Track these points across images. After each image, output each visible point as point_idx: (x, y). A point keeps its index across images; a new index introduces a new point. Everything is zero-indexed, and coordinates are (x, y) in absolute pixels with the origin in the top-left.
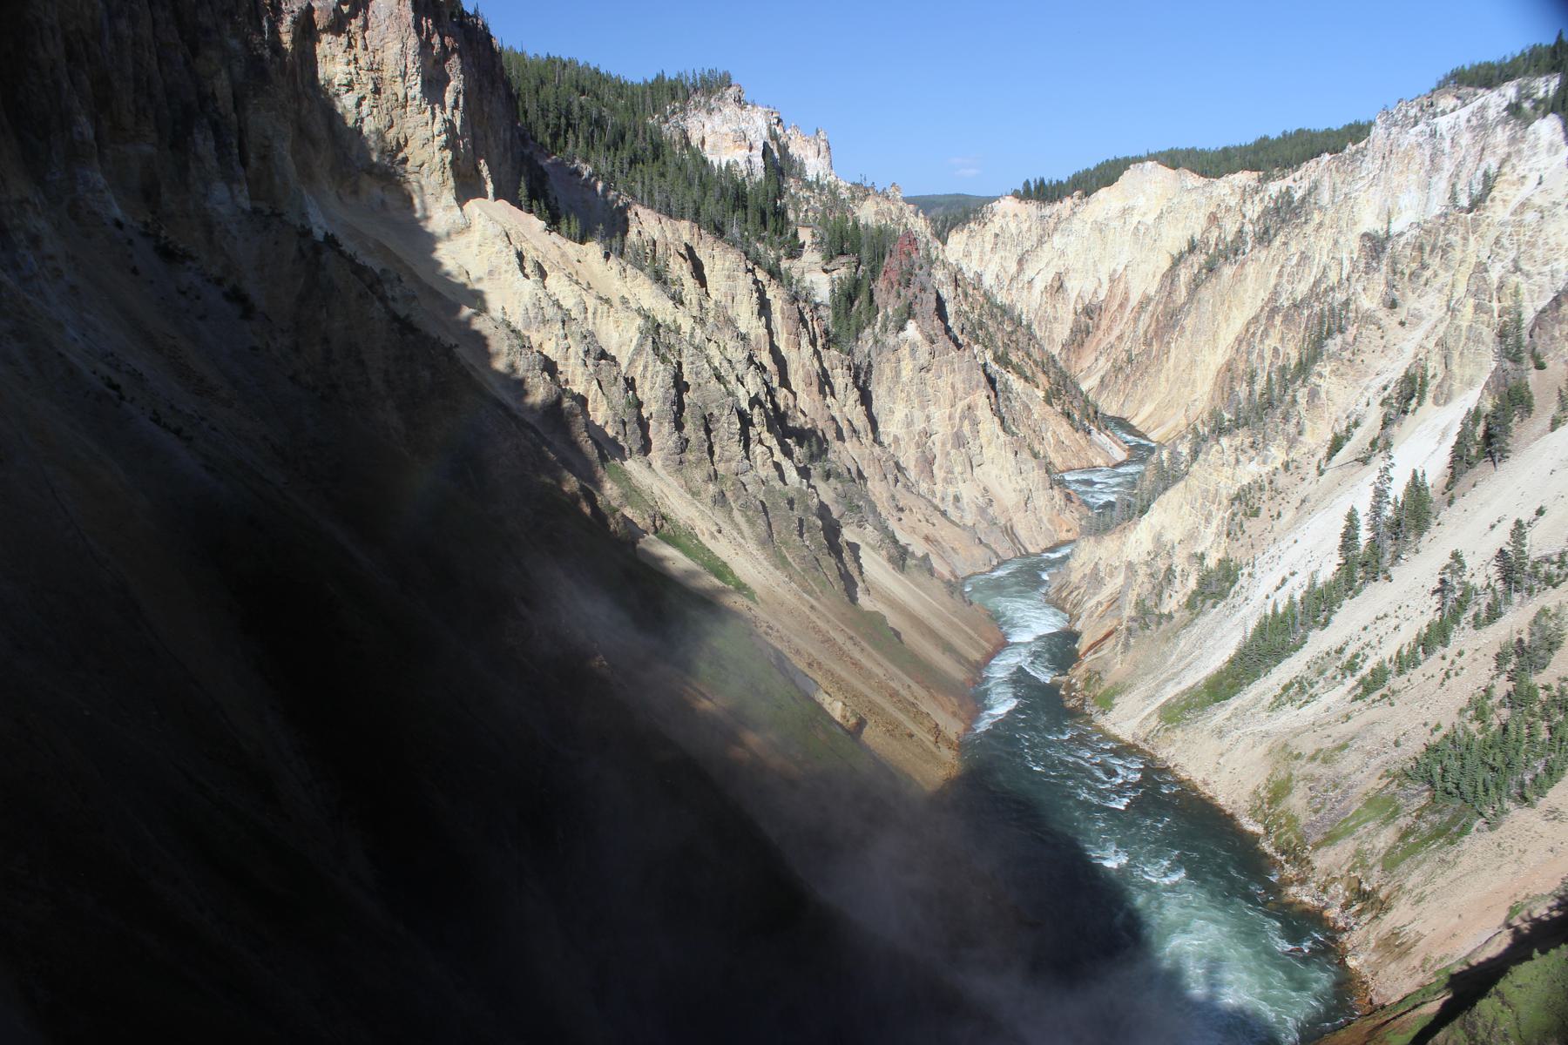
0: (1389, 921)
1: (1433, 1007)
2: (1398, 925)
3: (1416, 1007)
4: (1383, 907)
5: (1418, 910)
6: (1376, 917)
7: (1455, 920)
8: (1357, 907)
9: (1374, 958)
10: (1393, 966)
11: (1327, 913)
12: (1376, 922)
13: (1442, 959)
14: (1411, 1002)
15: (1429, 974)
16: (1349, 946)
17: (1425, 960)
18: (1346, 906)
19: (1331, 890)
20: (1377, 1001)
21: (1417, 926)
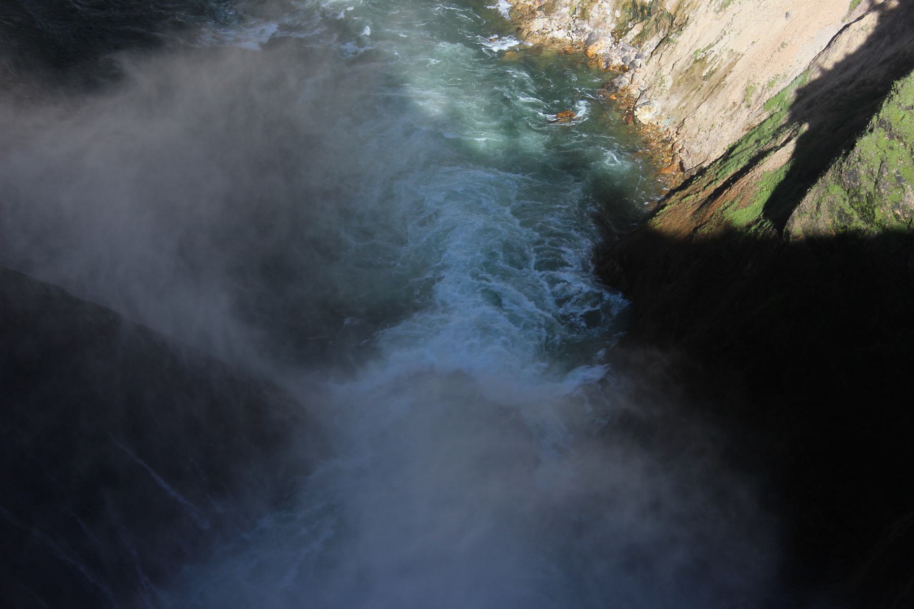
0: (686, 44)
1: (779, 160)
2: (701, 46)
3: (754, 161)
4: (675, 24)
5: (726, 17)
6: (665, 40)
7: (782, 22)
8: (636, 31)
9: (674, 102)
10: (704, 108)
11: (593, 50)
12: (666, 49)
13: (771, 84)
14: (744, 158)
15: (756, 109)
16: (635, 92)
17: (748, 91)
18: (619, 33)
19: (594, 13)
20: (688, 164)
21: (730, 42)
